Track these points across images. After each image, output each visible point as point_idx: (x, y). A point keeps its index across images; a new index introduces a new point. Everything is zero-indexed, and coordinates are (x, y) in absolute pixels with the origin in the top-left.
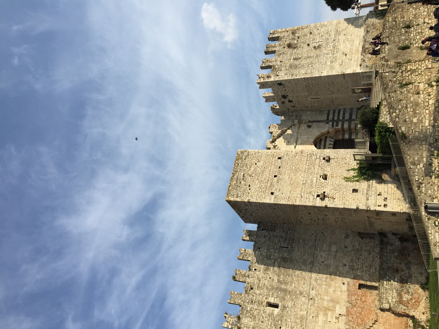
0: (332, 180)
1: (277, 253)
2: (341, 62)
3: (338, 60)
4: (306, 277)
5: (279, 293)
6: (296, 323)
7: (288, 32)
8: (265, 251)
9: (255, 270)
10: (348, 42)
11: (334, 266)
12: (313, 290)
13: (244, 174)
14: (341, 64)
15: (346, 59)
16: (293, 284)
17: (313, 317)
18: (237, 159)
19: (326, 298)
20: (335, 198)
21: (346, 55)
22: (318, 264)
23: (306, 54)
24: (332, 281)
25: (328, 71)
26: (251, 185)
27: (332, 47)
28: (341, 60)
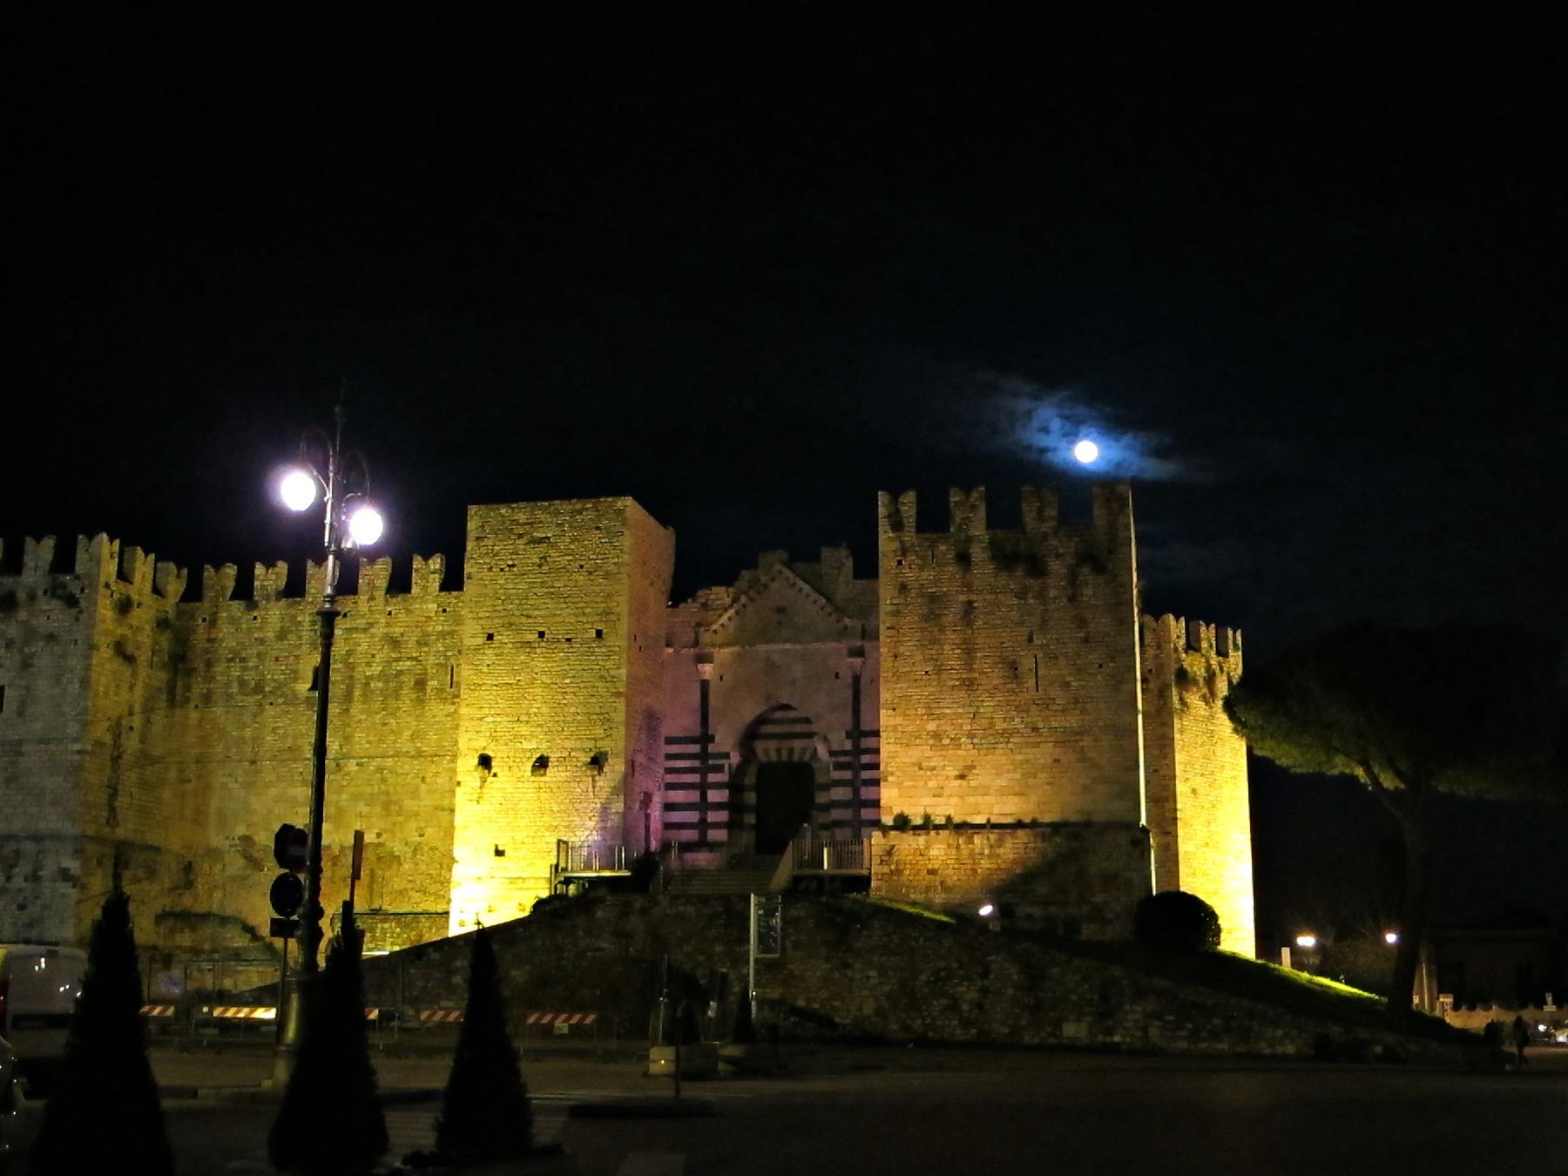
0: (530, 791)
1: (436, 661)
2: (932, 764)
3: (944, 753)
4: (385, 746)
5: (341, 687)
6: (285, 735)
8: (440, 628)
9: (390, 613)
11: (416, 809)
12: (358, 764)
13: (549, 538)
14: (925, 764)
16: (364, 716)
17: (301, 773)
19: (344, 796)
20: (481, 802)
21: (962, 777)
22: (418, 770)
23: (988, 640)
24: (383, 809)
25: (900, 729)
26: (515, 569)
27: (1005, 726)
28: (942, 764)
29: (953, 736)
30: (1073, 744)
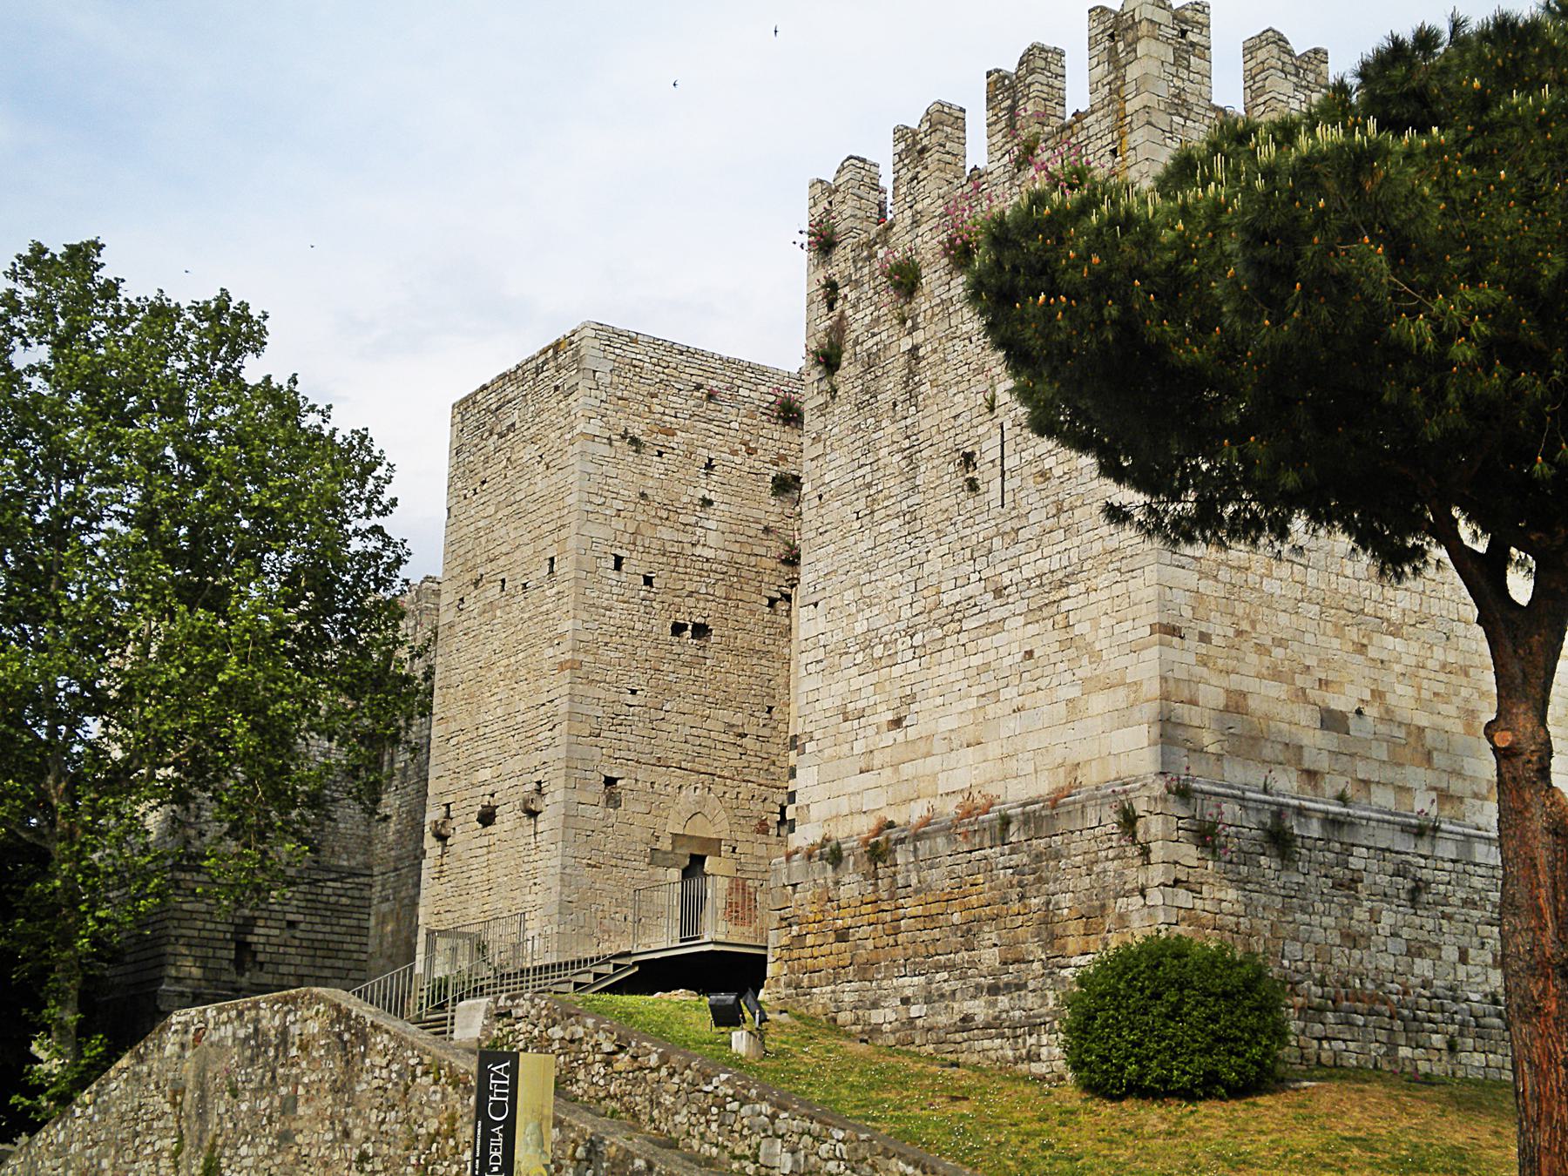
2: (861, 705)
7: (1114, 152)
10: (972, 703)
15: (871, 731)
18: (556, 347)
21: (897, 723)
27: (957, 595)
29: (887, 638)
30: (1054, 609)
